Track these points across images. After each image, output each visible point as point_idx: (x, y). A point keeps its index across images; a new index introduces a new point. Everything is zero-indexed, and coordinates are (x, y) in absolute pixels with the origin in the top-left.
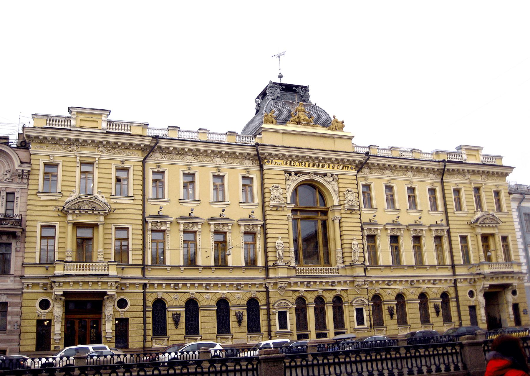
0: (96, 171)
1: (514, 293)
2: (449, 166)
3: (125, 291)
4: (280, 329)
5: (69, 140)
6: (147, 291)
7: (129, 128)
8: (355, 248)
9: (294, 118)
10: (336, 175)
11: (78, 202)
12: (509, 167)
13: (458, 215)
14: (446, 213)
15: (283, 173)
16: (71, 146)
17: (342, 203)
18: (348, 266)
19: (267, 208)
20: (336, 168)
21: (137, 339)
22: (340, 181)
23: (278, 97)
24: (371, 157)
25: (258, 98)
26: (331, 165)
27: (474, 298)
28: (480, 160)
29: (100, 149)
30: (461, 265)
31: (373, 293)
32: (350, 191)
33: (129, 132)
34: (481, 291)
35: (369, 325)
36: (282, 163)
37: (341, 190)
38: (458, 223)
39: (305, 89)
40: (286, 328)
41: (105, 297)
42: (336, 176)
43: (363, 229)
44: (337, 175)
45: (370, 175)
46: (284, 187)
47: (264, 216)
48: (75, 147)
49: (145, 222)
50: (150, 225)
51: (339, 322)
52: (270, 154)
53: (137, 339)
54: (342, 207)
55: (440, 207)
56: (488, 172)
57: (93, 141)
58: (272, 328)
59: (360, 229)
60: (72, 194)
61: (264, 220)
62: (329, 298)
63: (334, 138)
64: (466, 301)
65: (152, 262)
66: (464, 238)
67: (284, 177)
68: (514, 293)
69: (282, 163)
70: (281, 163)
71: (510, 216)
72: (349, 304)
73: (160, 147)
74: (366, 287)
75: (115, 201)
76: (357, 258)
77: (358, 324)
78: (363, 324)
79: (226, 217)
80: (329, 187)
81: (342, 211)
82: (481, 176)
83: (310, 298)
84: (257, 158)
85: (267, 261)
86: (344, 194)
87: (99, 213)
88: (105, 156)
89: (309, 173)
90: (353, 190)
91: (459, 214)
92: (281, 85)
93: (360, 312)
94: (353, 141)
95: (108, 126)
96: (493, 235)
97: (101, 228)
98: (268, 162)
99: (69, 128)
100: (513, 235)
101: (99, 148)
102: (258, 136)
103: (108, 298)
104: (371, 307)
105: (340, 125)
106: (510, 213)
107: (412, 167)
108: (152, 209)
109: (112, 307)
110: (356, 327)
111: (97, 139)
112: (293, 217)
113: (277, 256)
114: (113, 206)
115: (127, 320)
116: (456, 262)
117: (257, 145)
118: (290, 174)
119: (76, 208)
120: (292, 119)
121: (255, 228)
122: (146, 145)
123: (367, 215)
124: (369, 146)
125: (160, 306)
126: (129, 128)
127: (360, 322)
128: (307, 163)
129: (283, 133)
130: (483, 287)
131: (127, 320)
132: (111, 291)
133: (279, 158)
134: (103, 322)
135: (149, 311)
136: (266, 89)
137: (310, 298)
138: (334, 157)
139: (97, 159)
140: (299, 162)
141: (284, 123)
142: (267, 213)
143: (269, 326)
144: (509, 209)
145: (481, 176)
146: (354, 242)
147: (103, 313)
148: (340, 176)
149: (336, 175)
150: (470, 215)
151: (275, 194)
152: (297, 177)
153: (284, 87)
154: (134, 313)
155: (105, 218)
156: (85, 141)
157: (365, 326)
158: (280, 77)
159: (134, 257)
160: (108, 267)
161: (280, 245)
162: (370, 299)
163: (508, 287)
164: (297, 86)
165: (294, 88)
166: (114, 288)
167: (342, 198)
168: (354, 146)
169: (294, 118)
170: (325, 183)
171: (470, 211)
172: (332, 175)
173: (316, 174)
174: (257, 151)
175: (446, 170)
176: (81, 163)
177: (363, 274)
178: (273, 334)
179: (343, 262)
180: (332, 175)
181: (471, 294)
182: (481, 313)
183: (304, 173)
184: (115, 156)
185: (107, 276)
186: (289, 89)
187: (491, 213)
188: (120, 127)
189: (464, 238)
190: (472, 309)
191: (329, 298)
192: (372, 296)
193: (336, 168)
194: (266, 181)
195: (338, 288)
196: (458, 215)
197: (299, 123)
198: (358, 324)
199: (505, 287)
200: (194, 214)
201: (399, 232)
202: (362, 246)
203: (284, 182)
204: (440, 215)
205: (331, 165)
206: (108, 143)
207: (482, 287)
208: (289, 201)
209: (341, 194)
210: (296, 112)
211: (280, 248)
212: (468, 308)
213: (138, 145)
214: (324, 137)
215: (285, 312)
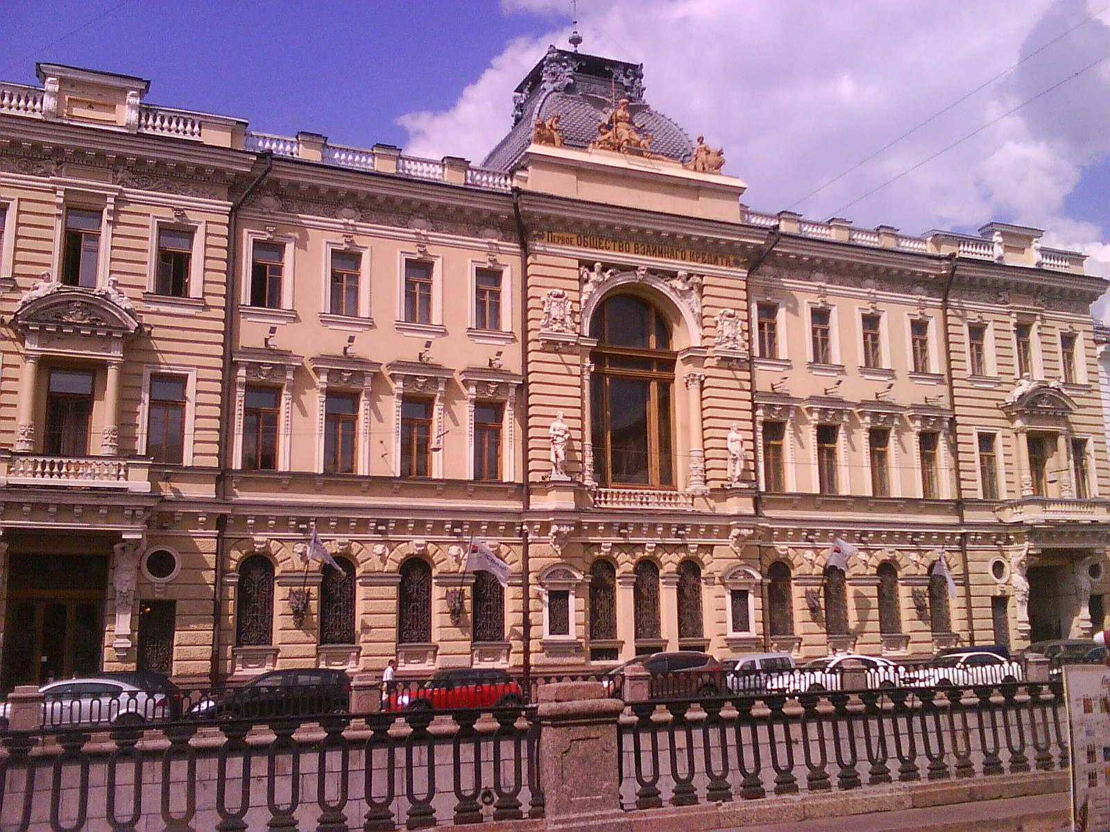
0: (106, 231)
1: (1094, 571)
2: (964, 272)
3: (172, 532)
4: (550, 634)
5: (37, 146)
6: (229, 533)
7: (196, 128)
8: (735, 448)
9: (606, 137)
10: (698, 275)
11: (56, 305)
12: (1101, 279)
16: (42, 163)
17: (707, 342)
18: (718, 490)
19: (531, 346)
20: (700, 259)
21: (196, 651)
22: (706, 290)
23: (569, 85)
24: (783, 239)
25: (519, 90)
26: (688, 253)
27: (1004, 580)
28: (1031, 258)
29: (119, 175)
31: (773, 558)
32: (730, 316)
33: (196, 138)
34: (1020, 565)
35: (761, 631)
36: (575, 241)
37: (706, 311)
39: (634, 71)
40: (567, 633)
41: (117, 546)
42: (698, 279)
43: (755, 408)
44: (702, 276)
46: (575, 296)
47: (525, 363)
48: (54, 167)
49: (230, 367)
50: (242, 372)
52: (546, 218)
53: (196, 651)
54: (709, 352)
55: (936, 365)
56: (1051, 289)
57: (101, 155)
58: (533, 632)
59: (749, 405)
60: (41, 283)
61: (526, 373)
64: (985, 586)
65: (243, 466)
66: (986, 440)
67: (576, 274)
68: (1094, 571)
69: (575, 241)
70: (569, 242)
71: (1094, 394)
72: (717, 581)
73: (276, 182)
74: (757, 542)
75: (154, 308)
76: (738, 473)
77: (735, 629)
78: (747, 630)
79: (432, 361)
80: (682, 305)
82: (1035, 297)
84: (514, 223)
85: (526, 472)
86: (717, 322)
87: (109, 334)
88: (132, 193)
89: (636, 268)
90: (737, 313)
92: (576, 57)
94: (743, 199)
95: (143, 121)
96: (1054, 436)
97: (112, 373)
98: (541, 237)
99: (38, 116)
100: (1099, 438)
101: (117, 172)
102: (519, 173)
103: (123, 548)
104: (766, 588)
105: (712, 159)
106: (1094, 386)
107: (876, 268)
108: (252, 331)
109: (134, 572)
110: (732, 635)
111: (113, 150)
112: (592, 369)
113: (553, 458)
114: (146, 319)
115: (172, 604)
117: (516, 190)
118: (592, 269)
119: (50, 318)
120: (600, 138)
121: (501, 391)
123: (766, 377)
124: (779, 214)
125: (259, 566)
126: (196, 128)
127: (741, 622)
128: (632, 245)
130: (1028, 555)
131: (172, 604)
132: (133, 533)
133: (567, 230)
134: (109, 611)
135: (231, 584)
136: (540, 67)
139: (111, 200)
140: (614, 241)
141: (583, 148)
142: (531, 357)
143: (527, 624)
144: (1094, 377)
145: (1035, 297)
146: (732, 435)
147: (110, 589)
148: (706, 280)
149: (698, 275)
150: (1005, 387)
151: (554, 313)
155: (126, 350)
156: (80, 153)
158: (576, 41)
159: (197, 449)
160: (126, 471)
161: (561, 433)
162: (766, 570)
163: (1083, 557)
164: (615, 64)
166: (138, 526)
167: (708, 331)
168: (744, 211)
169: (606, 137)
170: (672, 296)
171: (1005, 378)
172: (690, 276)
173: (652, 272)
174: (516, 207)
175: (955, 278)
176: (68, 208)
177: (752, 512)
178: (534, 645)
179: (706, 482)
181: (998, 568)
182: (1018, 615)
183: (624, 268)
184: (162, 196)
186: (595, 68)
187: (1053, 384)
188: (174, 124)
189: (986, 440)
190: (1000, 603)
191: (670, 563)
192: (769, 564)
193: (700, 259)
194: (530, 281)
195: (693, 543)
197: (617, 148)
198: (735, 629)
199: (1075, 556)
200: (354, 350)
201: (837, 417)
202: (750, 445)
203: (576, 285)
205: (688, 253)
206: (141, 161)
207: (1024, 553)
208: (586, 331)
209: (706, 321)
210: (611, 121)
211: (560, 440)
212: (989, 602)
213: (219, 172)
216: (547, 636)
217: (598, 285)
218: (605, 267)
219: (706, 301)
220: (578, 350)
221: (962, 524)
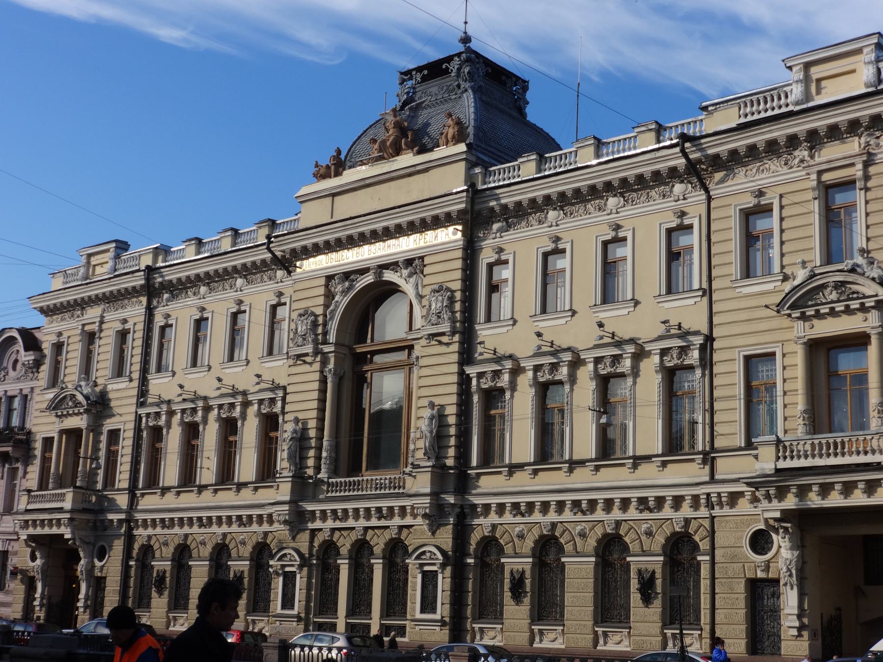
6: (135, 532)
13: (746, 290)
14: (708, 292)
15: (323, 281)
22: (427, 270)
30: (740, 449)
38: (743, 316)
40: (293, 609)
44: (422, 258)
45: (509, 236)
51: (395, 602)
52: (293, 251)
62: (379, 543)
63: (426, 170)
77: (422, 611)
78: (434, 610)
81: (423, 342)
83: (345, 545)
91: (753, 287)
93: (429, 580)
116: (718, 444)
122: (141, 286)
129: (334, 195)
137: (345, 545)
138: (403, 220)
148: (427, 260)
152: (347, 284)
153: (426, 72)
154: (111, 568)
157: (437, 616)
165: (444, 67)
170: (400, 282)
180: (409, 262)
183: (363, 271)
185: (60, 510)
191: (379, 543)
196: (746, 290)
198: (422, 611)
204: (691, 301)
208: (332, 338)
209: (425, 302)
214: (410, 175)
215: (293, 574)
216: (279, 610)
217: (345, 292)
218: (347, 276)
219: (426, 281)
220: (318, 359)
221: (713, 480)
